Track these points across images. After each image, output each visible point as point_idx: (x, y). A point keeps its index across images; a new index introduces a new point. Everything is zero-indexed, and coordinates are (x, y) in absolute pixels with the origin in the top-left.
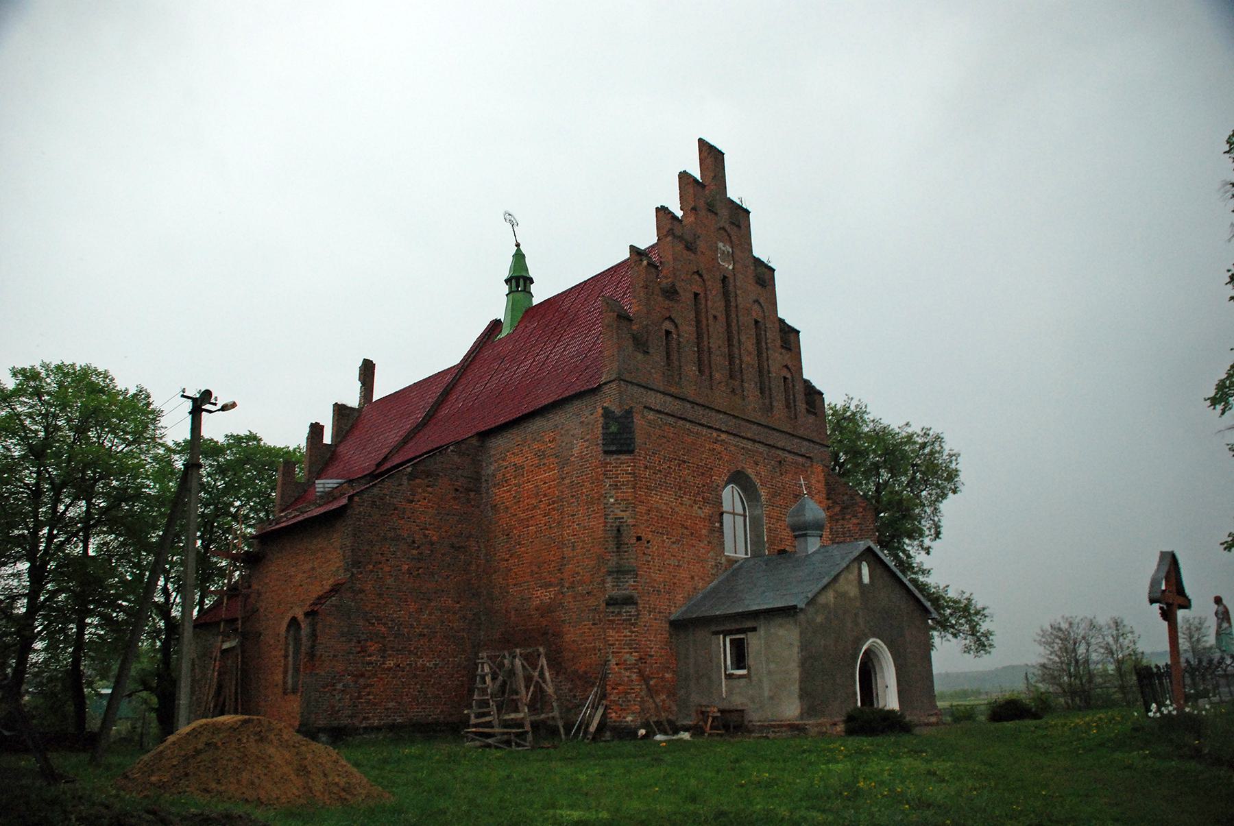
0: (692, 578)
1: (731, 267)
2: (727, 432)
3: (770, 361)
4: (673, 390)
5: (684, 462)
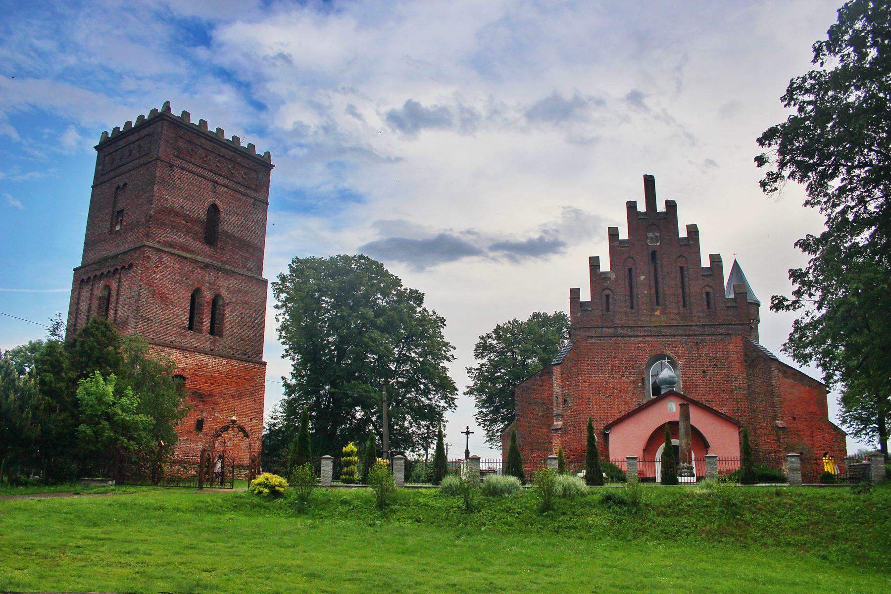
0: (621, 412)
1: (658, 244)
2: (651, 336)
3: (691, 288)
4: (608, 324)
5: (615, 358)
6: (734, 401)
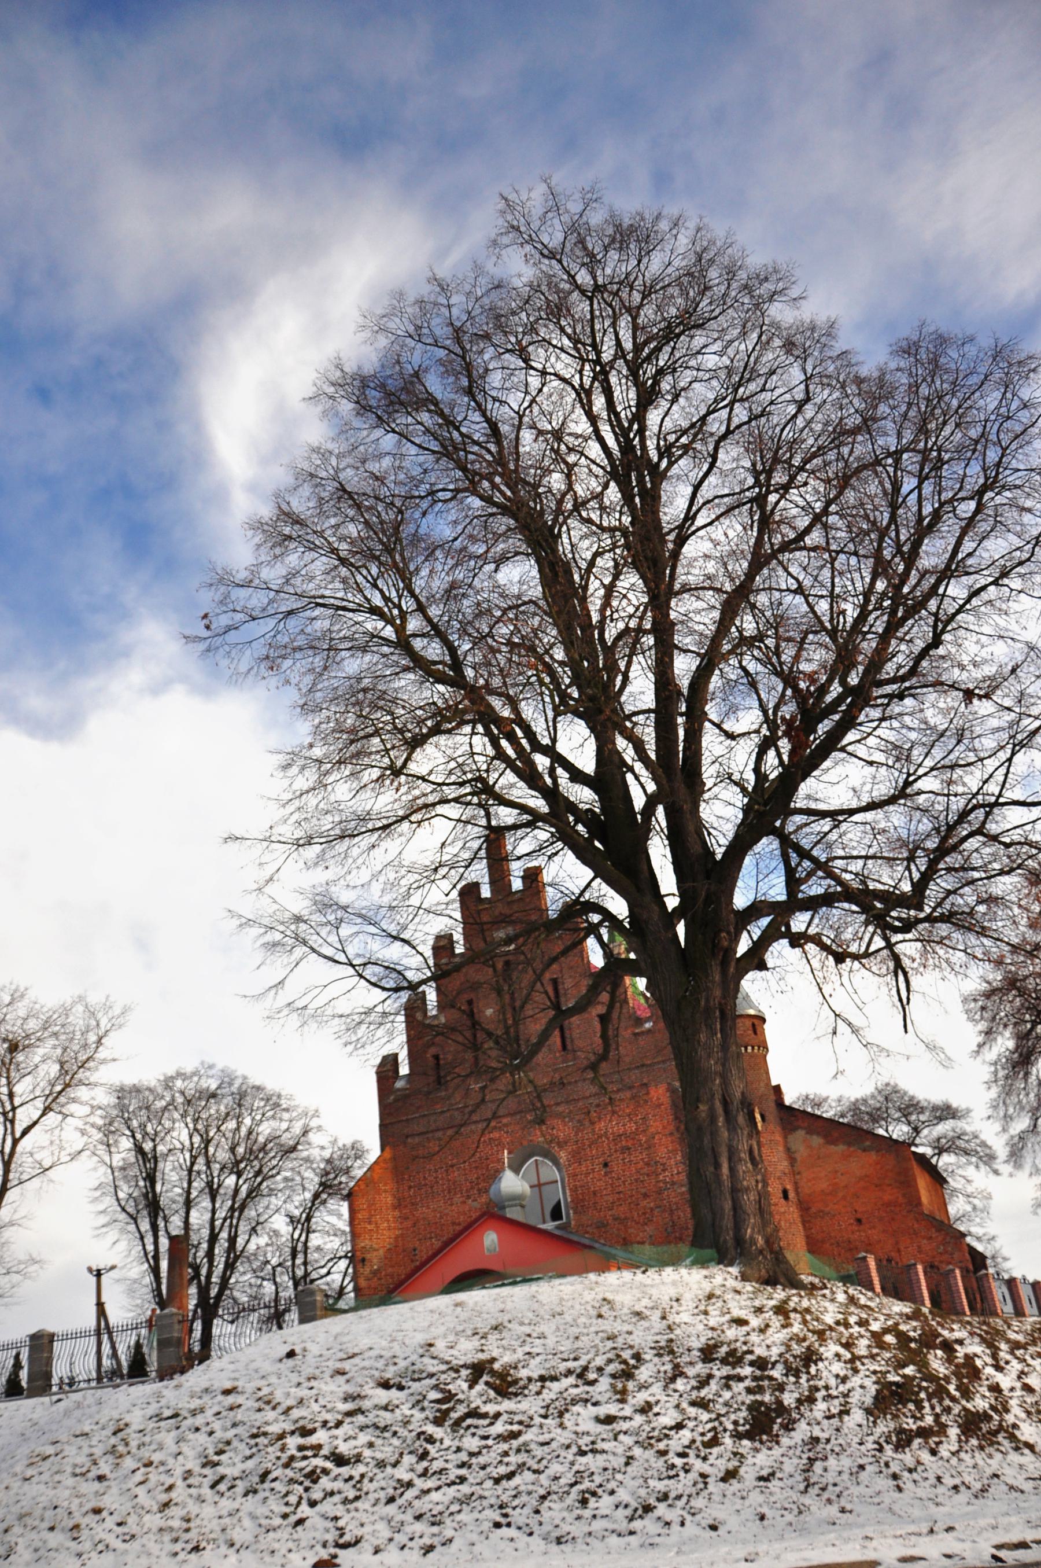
6: (664, 1211)
